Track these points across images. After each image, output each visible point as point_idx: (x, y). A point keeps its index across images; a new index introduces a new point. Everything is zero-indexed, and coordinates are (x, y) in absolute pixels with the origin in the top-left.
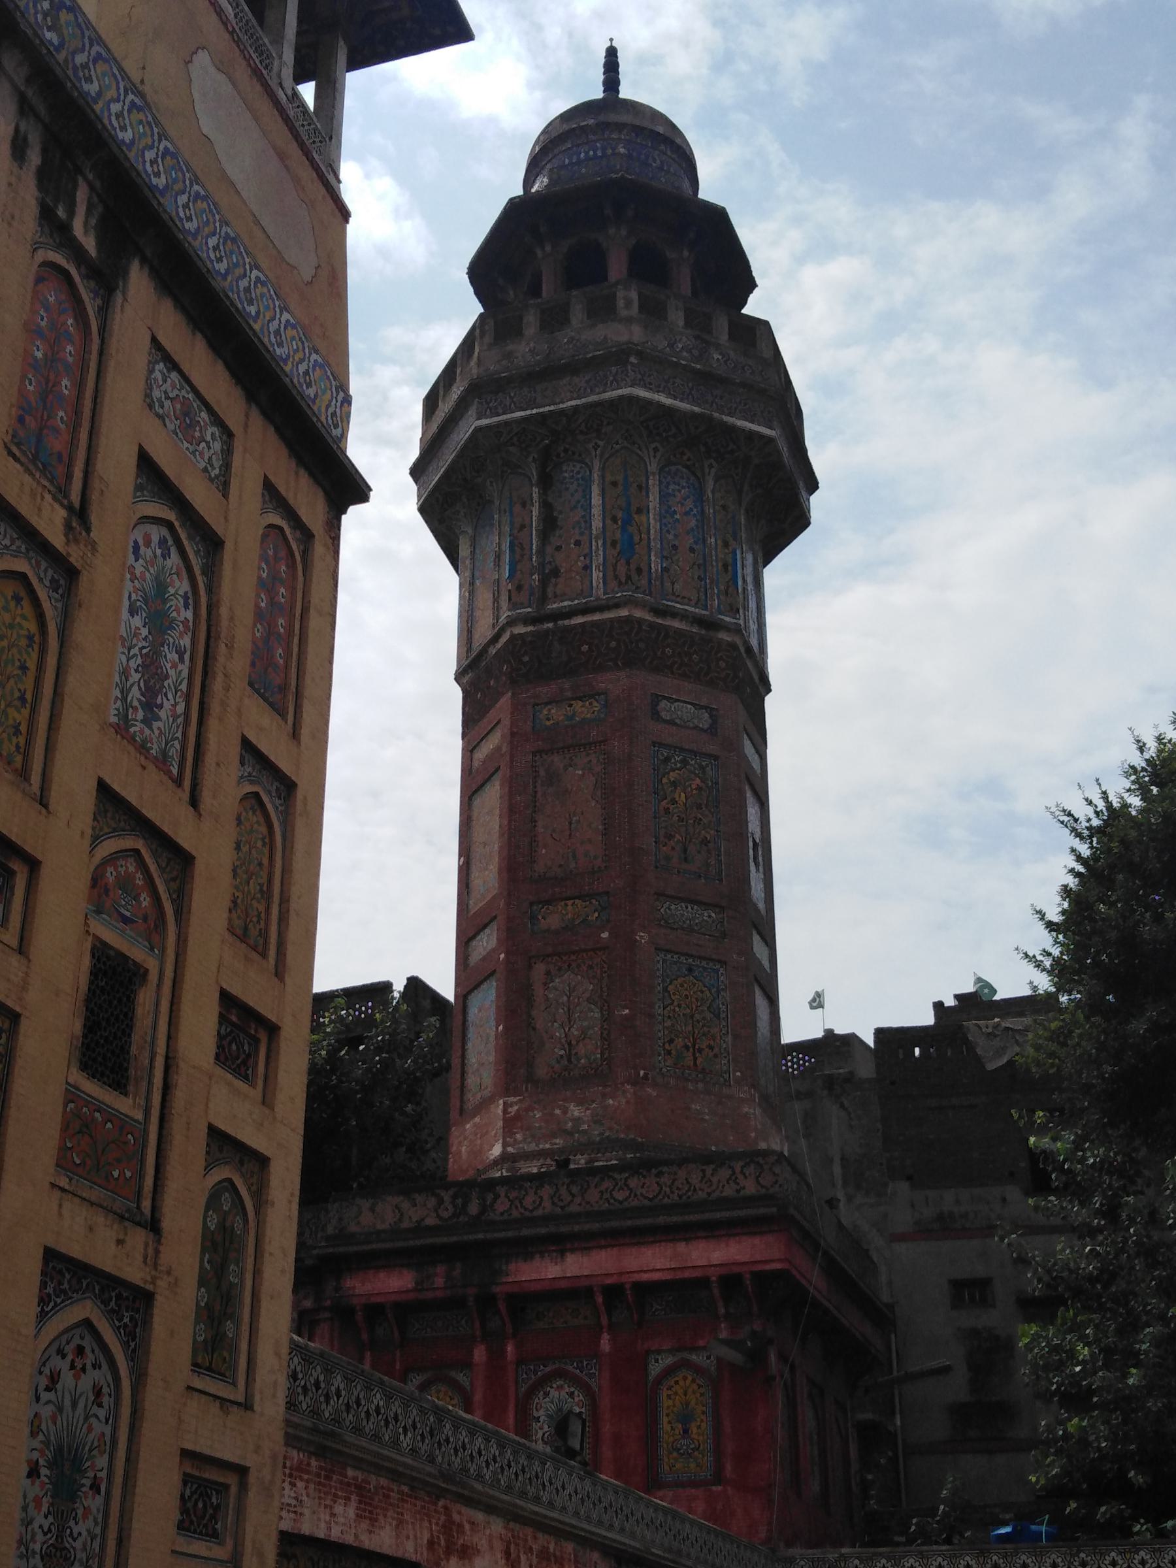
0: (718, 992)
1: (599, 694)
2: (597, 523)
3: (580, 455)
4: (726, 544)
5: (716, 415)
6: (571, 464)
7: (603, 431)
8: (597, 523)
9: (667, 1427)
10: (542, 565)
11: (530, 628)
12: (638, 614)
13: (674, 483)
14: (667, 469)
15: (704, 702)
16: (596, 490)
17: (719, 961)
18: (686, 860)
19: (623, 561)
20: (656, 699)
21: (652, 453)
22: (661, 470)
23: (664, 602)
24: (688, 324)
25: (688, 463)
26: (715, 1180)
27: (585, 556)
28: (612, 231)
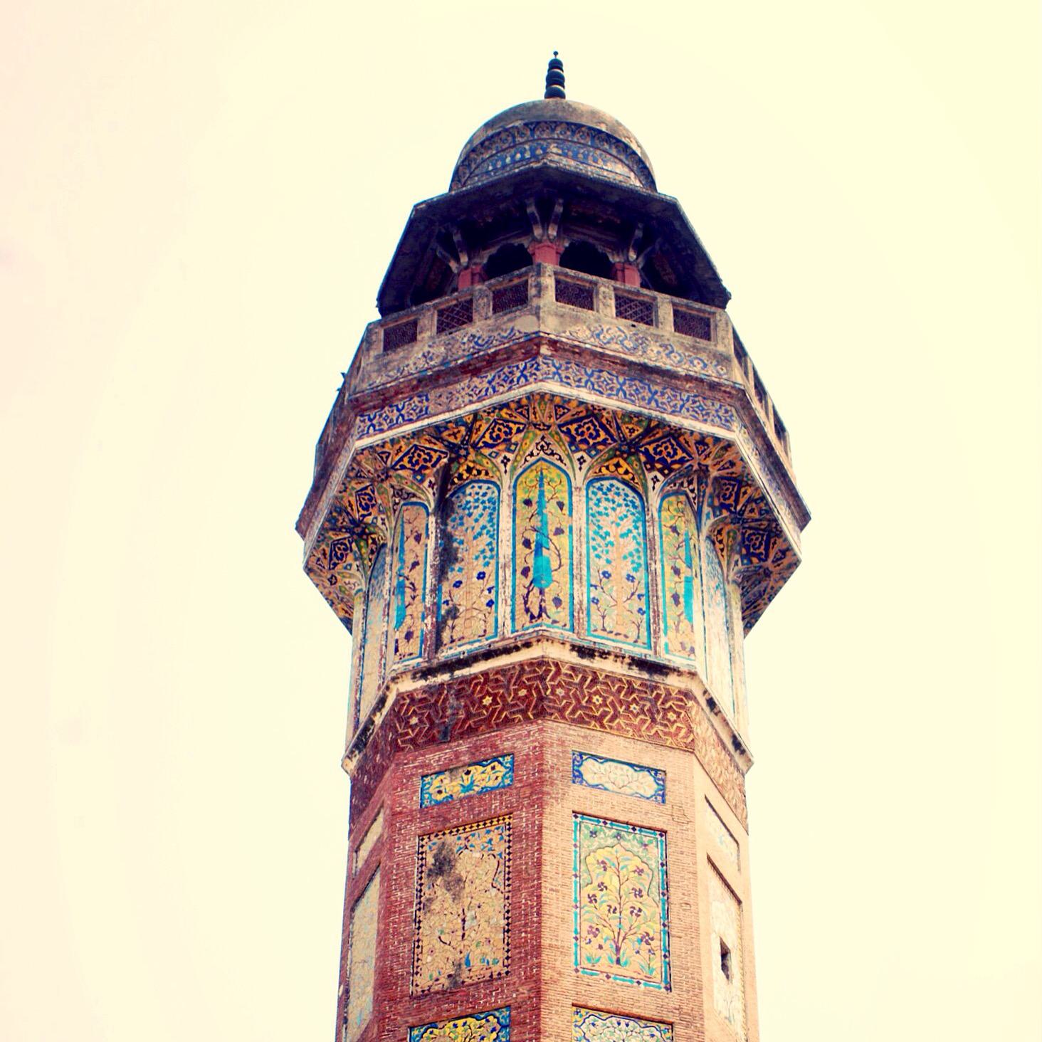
1: (504, 756)
2: (505, 550)
3: (487, 474)
6: (476, 485)
7: (513, 441)
8: (505, 550)
11: (422, 683)
13: (607, 500)
14: (597, 485)
16: (505, 511)
18: (618, 962)
21: (577, 465)
23: (589, 638)
25: (627, 477)
27: (490, 590)
28: (537, 232)
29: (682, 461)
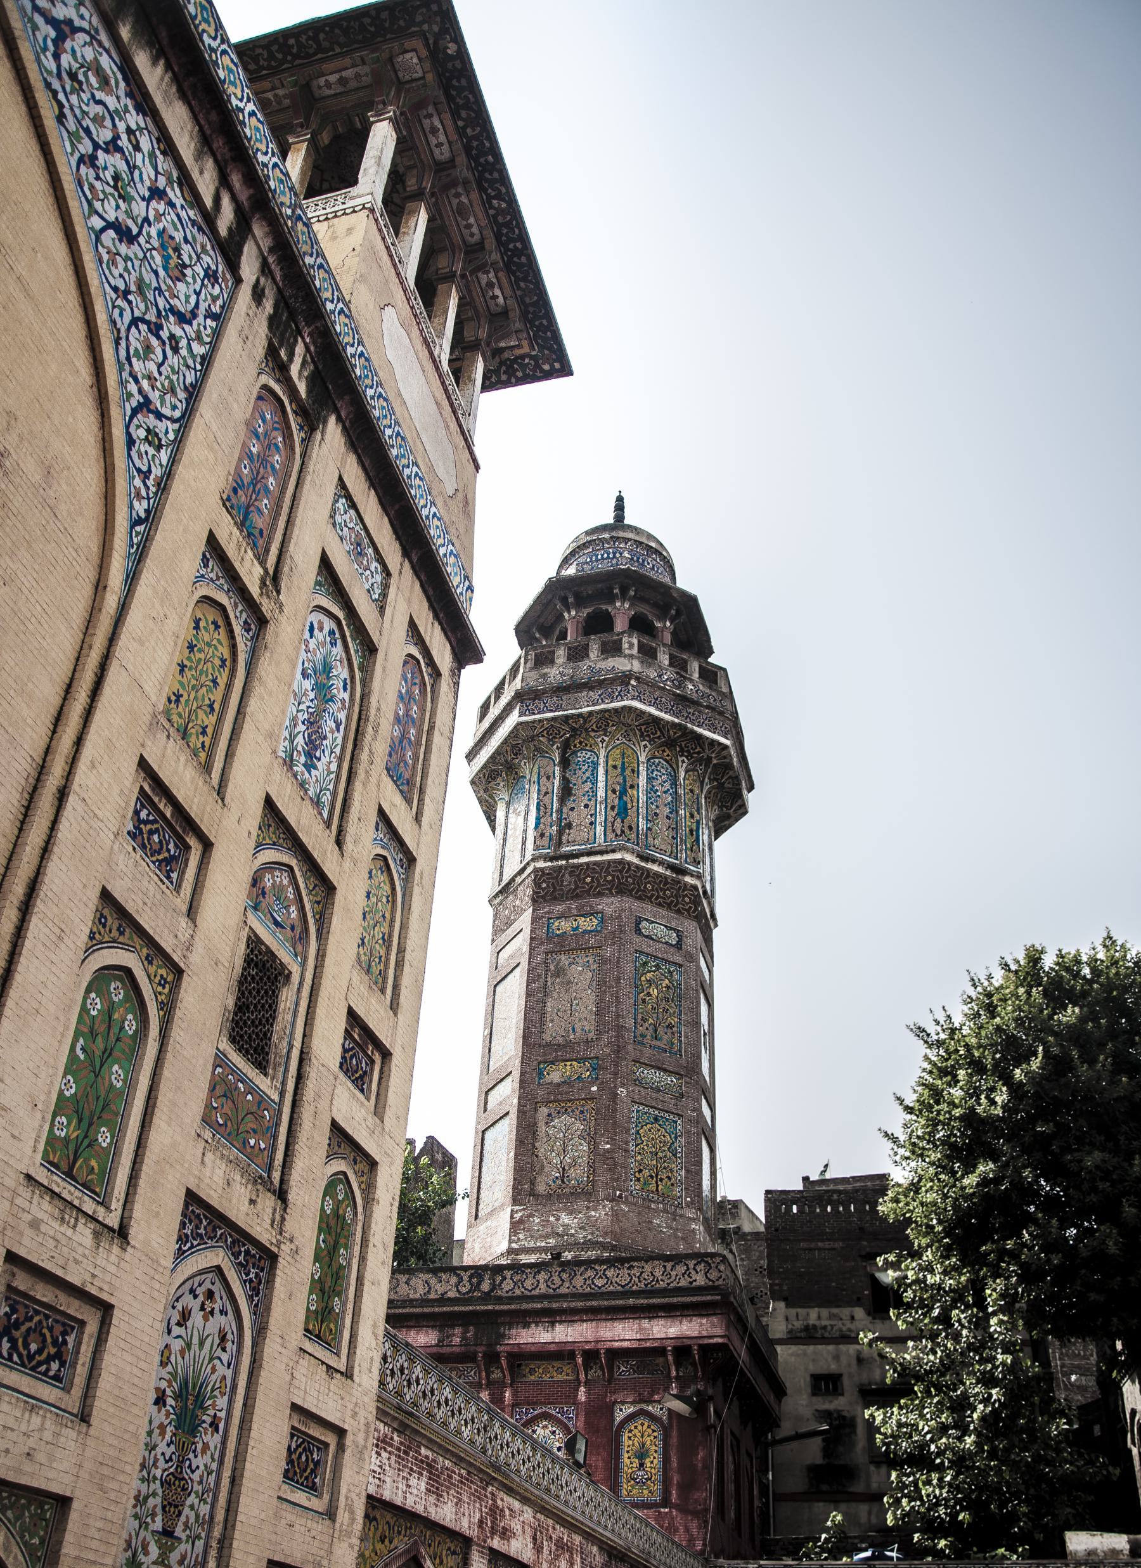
0: (676, 1138)
2: (601, 793)
4: (692, 816)
5: (689, 725)
8: (601, 793)
9: (627, 1461)
10: (560, 820)
11: (549, 864)
12: (629, 857)
15: (673, 925)
16: (601, 771)
17: (678, 1115)
19: (619, 820)
20: (639, 920)
22: (648, 760)
24: (671, 665)
26: (673, 1273)
28: (618, 604)
29: (699, 753)
